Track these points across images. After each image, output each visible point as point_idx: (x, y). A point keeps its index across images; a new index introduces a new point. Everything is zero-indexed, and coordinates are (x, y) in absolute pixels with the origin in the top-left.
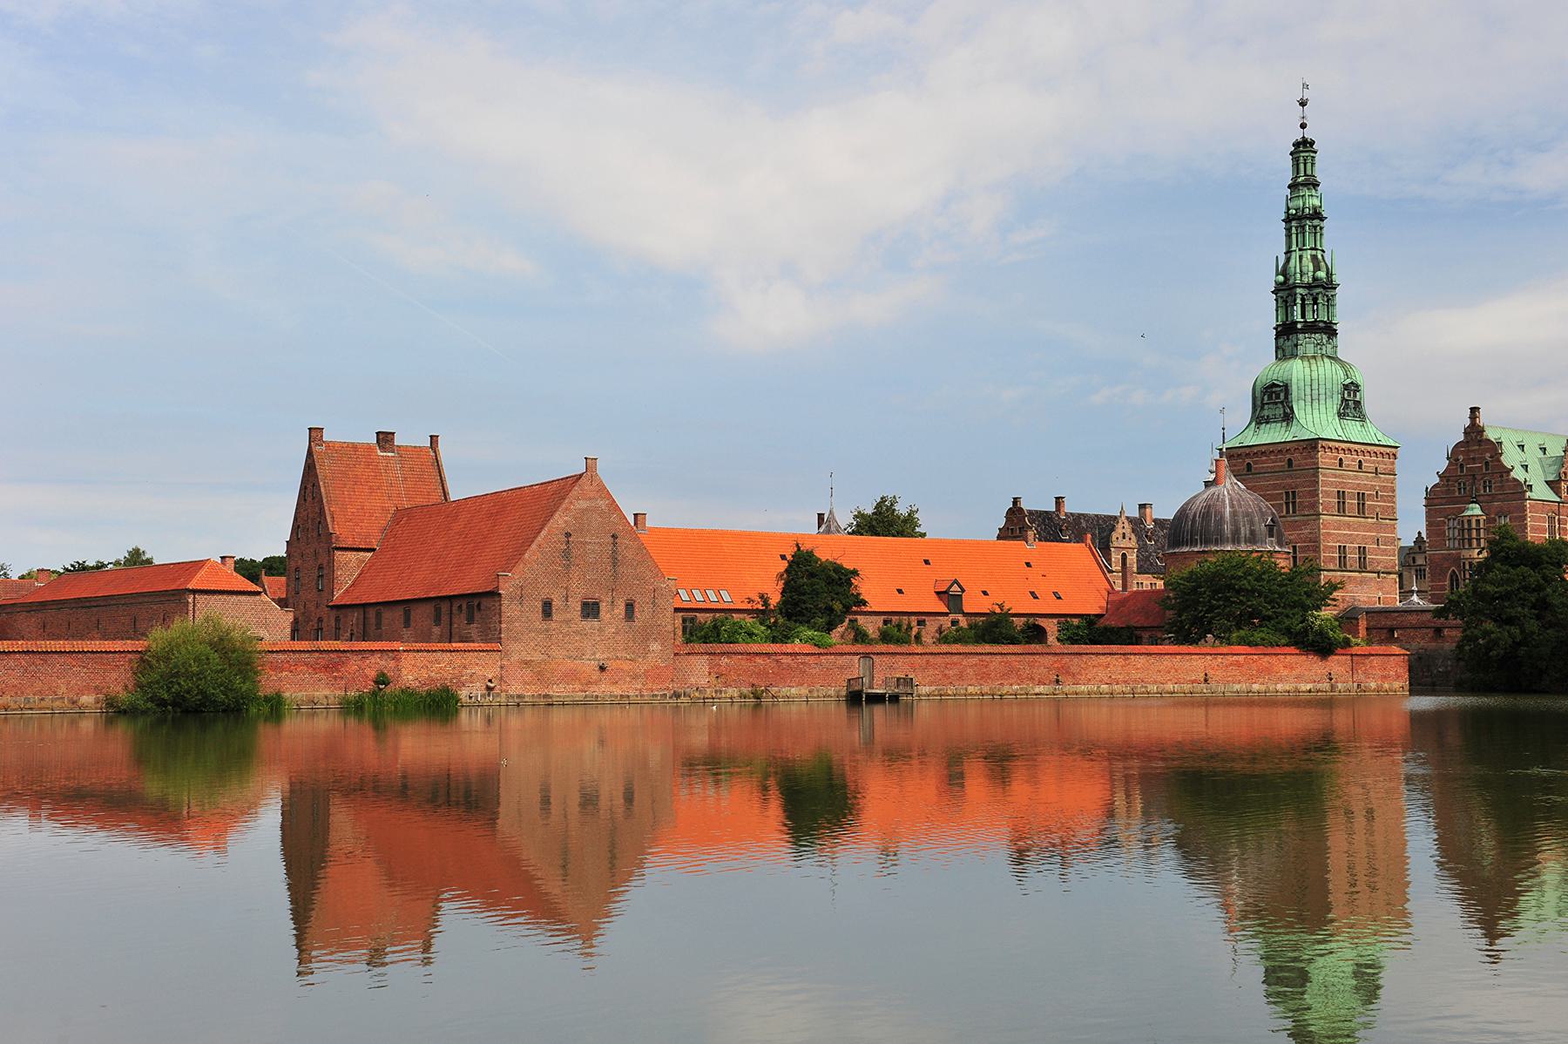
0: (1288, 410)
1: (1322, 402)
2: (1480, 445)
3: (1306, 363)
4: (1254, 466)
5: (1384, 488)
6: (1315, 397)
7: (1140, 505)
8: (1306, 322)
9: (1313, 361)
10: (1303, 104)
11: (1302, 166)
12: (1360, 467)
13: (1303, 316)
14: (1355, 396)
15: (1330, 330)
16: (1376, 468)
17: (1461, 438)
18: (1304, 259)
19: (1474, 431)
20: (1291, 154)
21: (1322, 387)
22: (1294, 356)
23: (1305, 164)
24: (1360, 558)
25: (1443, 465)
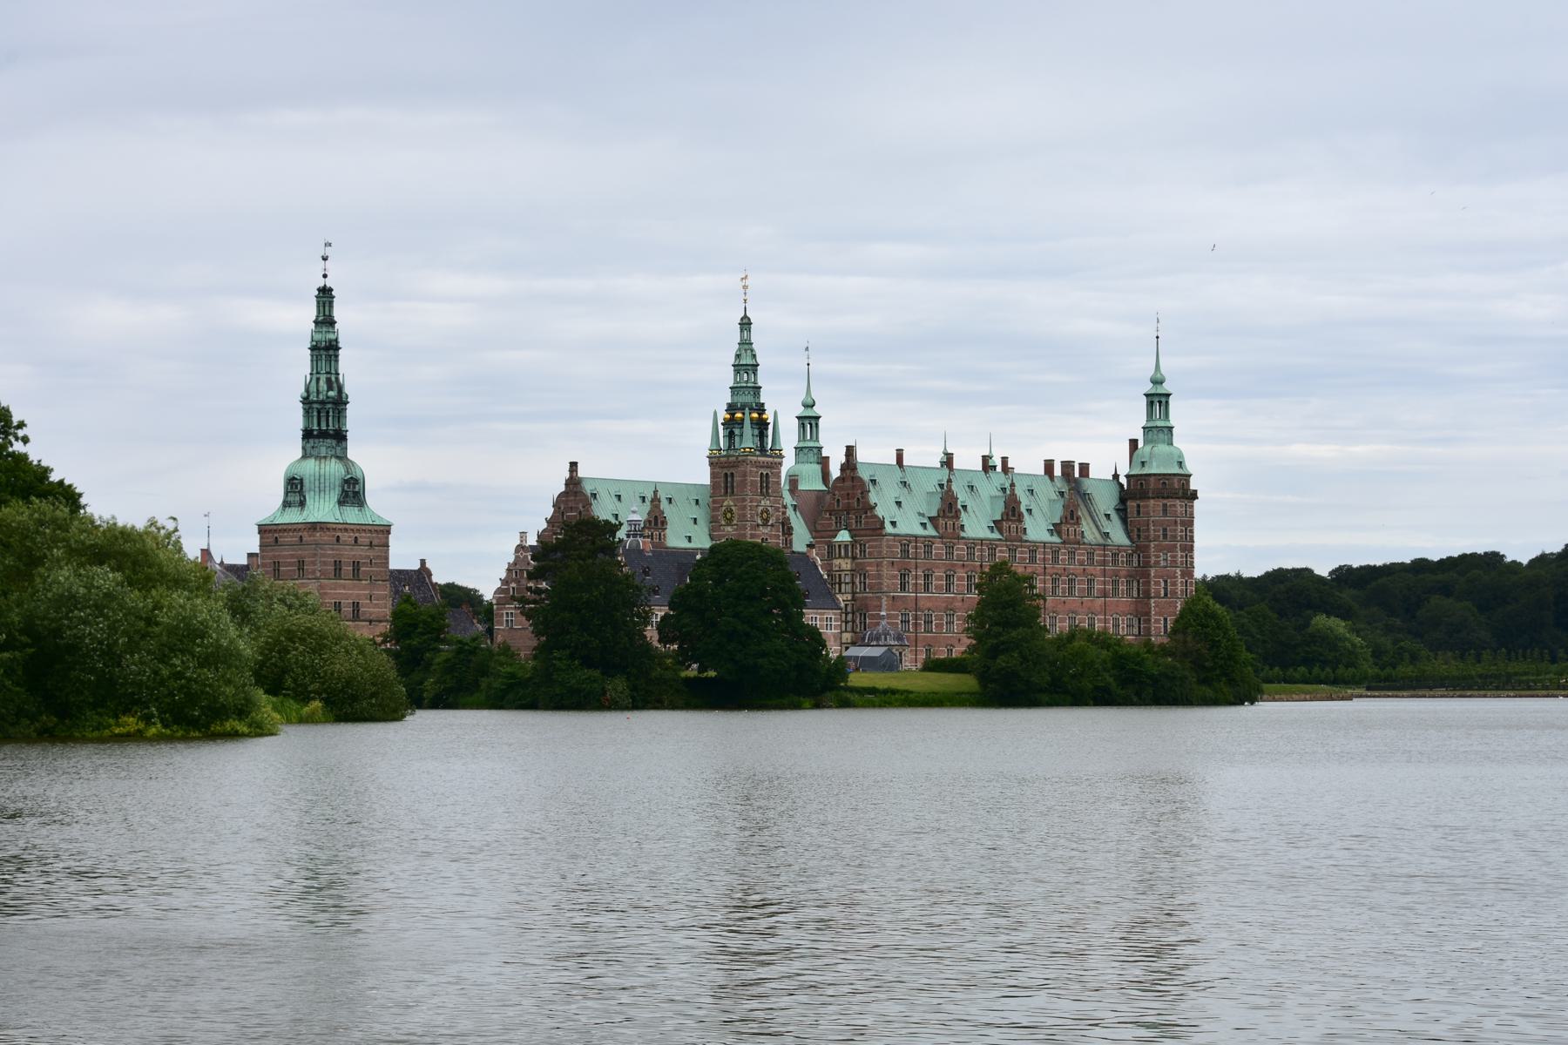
0: (302, 499)
1: (327, 492)
2: (576, 496)
3: (318, 462)
4: (279, 540)
5: (378, 557)
6: (322, 488)
7: (248, 554)
8: (320, 429)
9: (323, 461)
10: (325, 259)
11: (321, 309)
13: (319, 424)
14: (354, 487)
15: (340, 437)
16: (371, 543)
17: (562, 488)
19: (574, 483)
22: (311, 456)
24: (353, 611)
25: (549, 511)
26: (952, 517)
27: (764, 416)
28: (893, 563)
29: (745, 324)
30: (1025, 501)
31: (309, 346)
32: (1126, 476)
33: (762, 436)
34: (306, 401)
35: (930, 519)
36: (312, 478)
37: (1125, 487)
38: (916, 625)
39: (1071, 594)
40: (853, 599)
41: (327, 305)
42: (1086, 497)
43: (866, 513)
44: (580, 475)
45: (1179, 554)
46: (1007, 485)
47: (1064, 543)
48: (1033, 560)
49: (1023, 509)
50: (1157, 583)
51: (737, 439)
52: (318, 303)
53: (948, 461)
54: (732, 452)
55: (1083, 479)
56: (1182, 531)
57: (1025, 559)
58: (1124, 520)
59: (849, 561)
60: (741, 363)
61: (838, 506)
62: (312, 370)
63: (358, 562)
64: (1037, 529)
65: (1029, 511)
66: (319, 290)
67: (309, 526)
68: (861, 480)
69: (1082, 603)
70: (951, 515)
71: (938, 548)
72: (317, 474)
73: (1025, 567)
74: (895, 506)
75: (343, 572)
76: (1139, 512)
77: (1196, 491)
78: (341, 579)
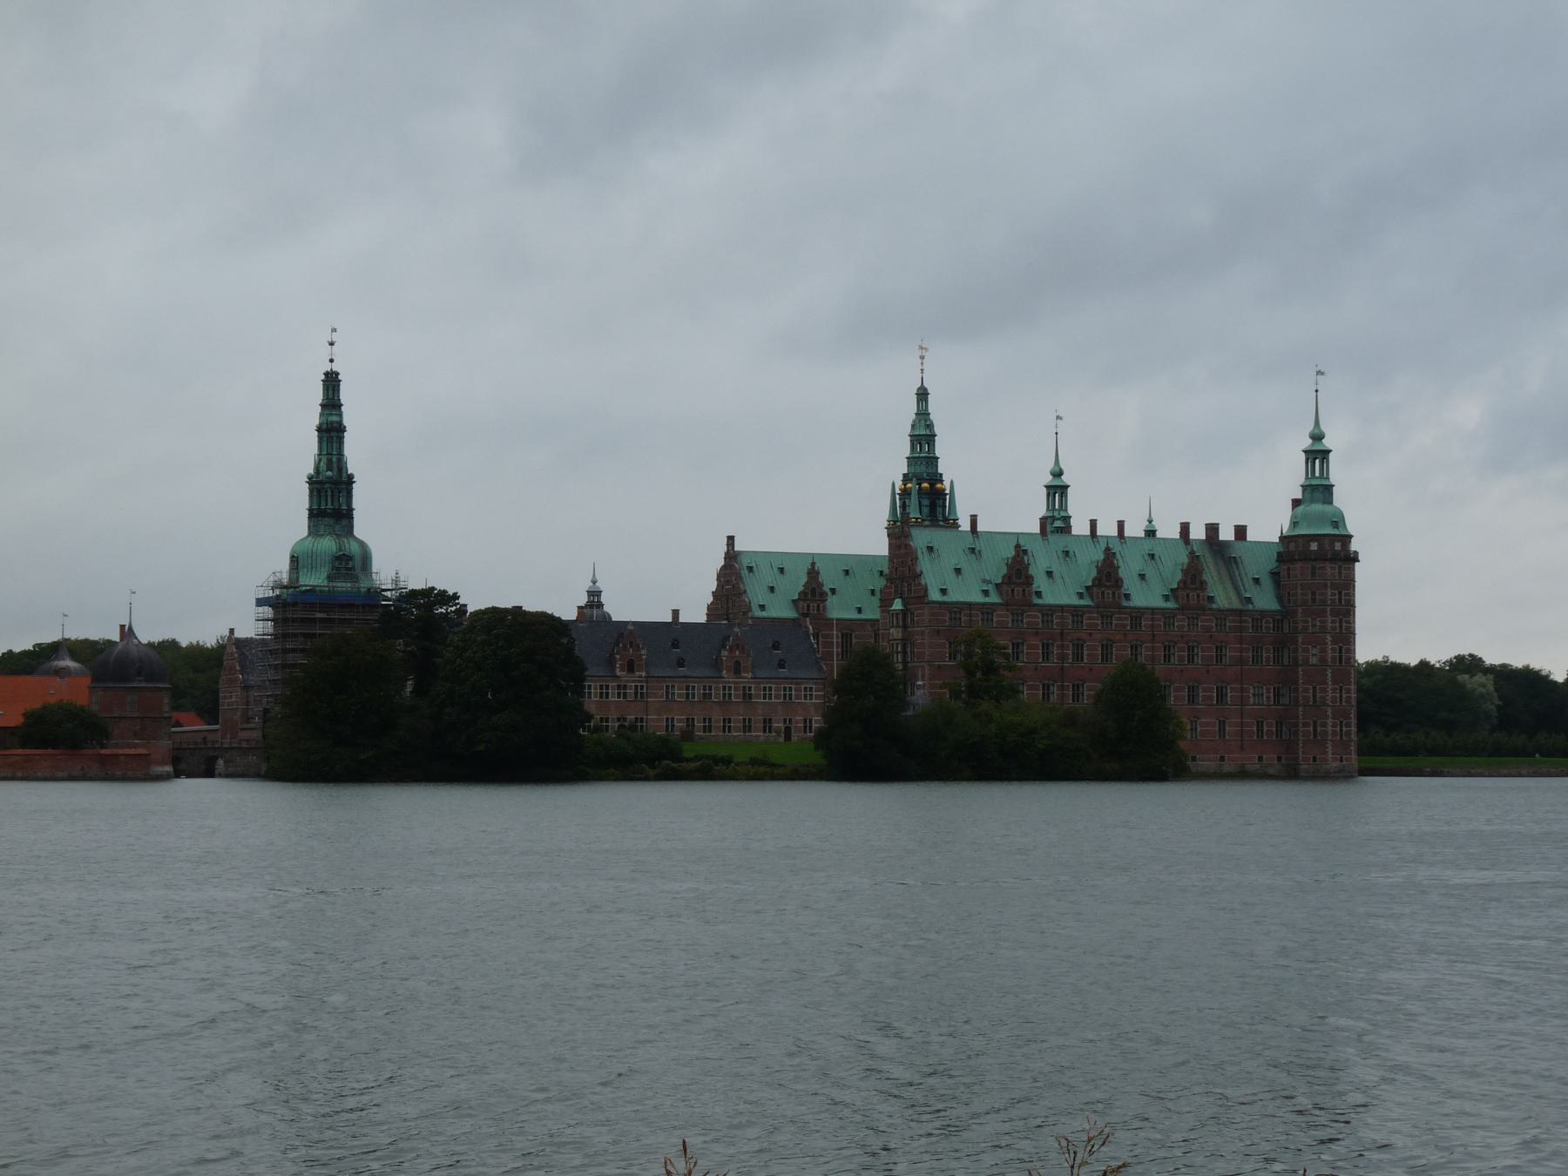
6: (314, 565)
10: (332, 344)
14: (348, 564)
17: (723, 563)
19: (732, 556)
20: (322, 381)
21: (319, 558)
26: (1023, 584)
28: (938, 631)
29: (923, 395)
44: (737, 548)
45: (1330, 619)
47: (1182, 609)
55: (1240, 544)
56: (1333, 595)
57: (1125, 626)
59: (900, 630)
70: (1018, 581)
73: (1125, 635)
74: (952, 575)
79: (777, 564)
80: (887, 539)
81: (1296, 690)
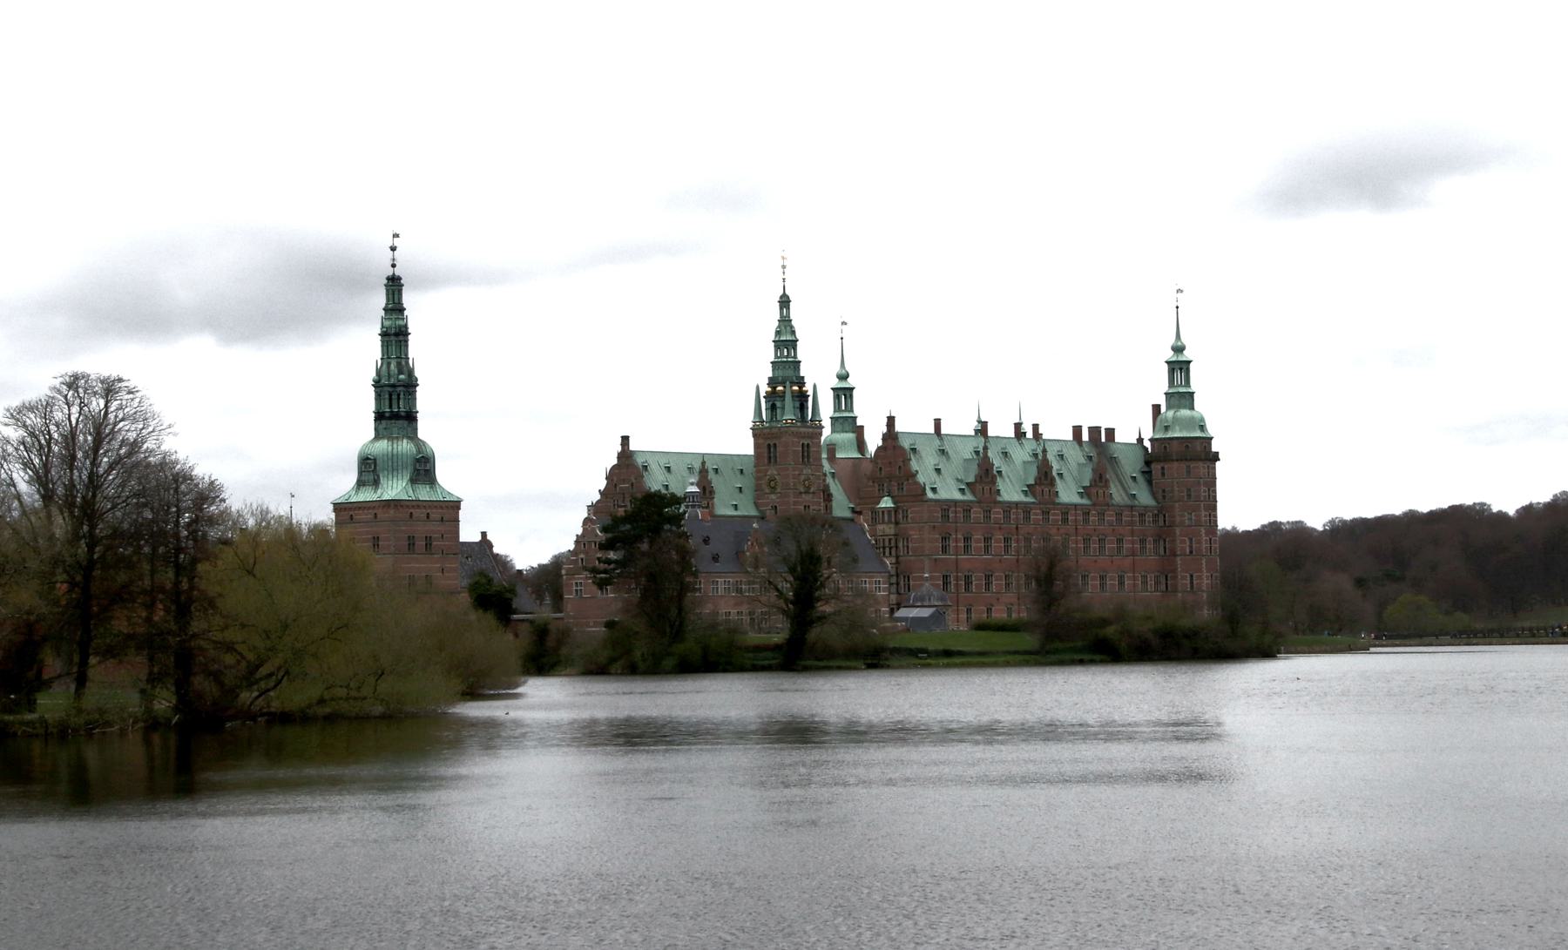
1: (400, 471)
3: (390, 443)
4: (354, 517)
8: (392, 412)
9: (395, 441)
10: (393, 249)
12: (428, 517)
13: (391, 407)
15: (411, 417)
17: (615, 462)
18: (392, 365)
19: (626, 455)
20: (385, 285)
22: (383, 438)
23: (394, 294)
25: (602, 484)
27: (804, 389)
28: (934, 527)
29: (785, 302)
30: (1055, 466)
31: (379, 332)
32: (1151, 440)
33: (803, 407)
34: (377, 384)
35: (968, 484)
36: (386, 459)
37: (1150, 450)
38: (957, 585)
39: (1102, 548)
40: (897, 562)
41: (396, 293)
42: (1113, 460)
43: (908, 480)
44: (631, 448)
45: (1203, 513)
46: (1039, 451)
47: (1094, 505)
48: (1065, 520)
49: (1054, 473)
50: (1184, 542)
51: (778, 411)
52: (387, 291)
53: (982, 429)
54: (774, 424)
55: (1111, 444)
56: (1205, 491)
57: (1058, 521)
58: (1150, 482)
59: (892, 526)
60: (782, 339)
61: (881, 473)
62: (383, 355)
63: (430, 537)
64: (1068, 494)
65: (1060, 475)
66: (388, 279)
67: (384, 503)
68: (902, 449)
69: (1112, 562)
70: (987, 480)
71: (977, 513)
72: (390, 454)
73: (1058, 529)
74: (934, 474)
75: (416, 546)
76: (1163, 474)
77: (1218, 453)
78: (414, 554)
79: (663, 462)
80: (752, 439)
81: (1175, 578)
